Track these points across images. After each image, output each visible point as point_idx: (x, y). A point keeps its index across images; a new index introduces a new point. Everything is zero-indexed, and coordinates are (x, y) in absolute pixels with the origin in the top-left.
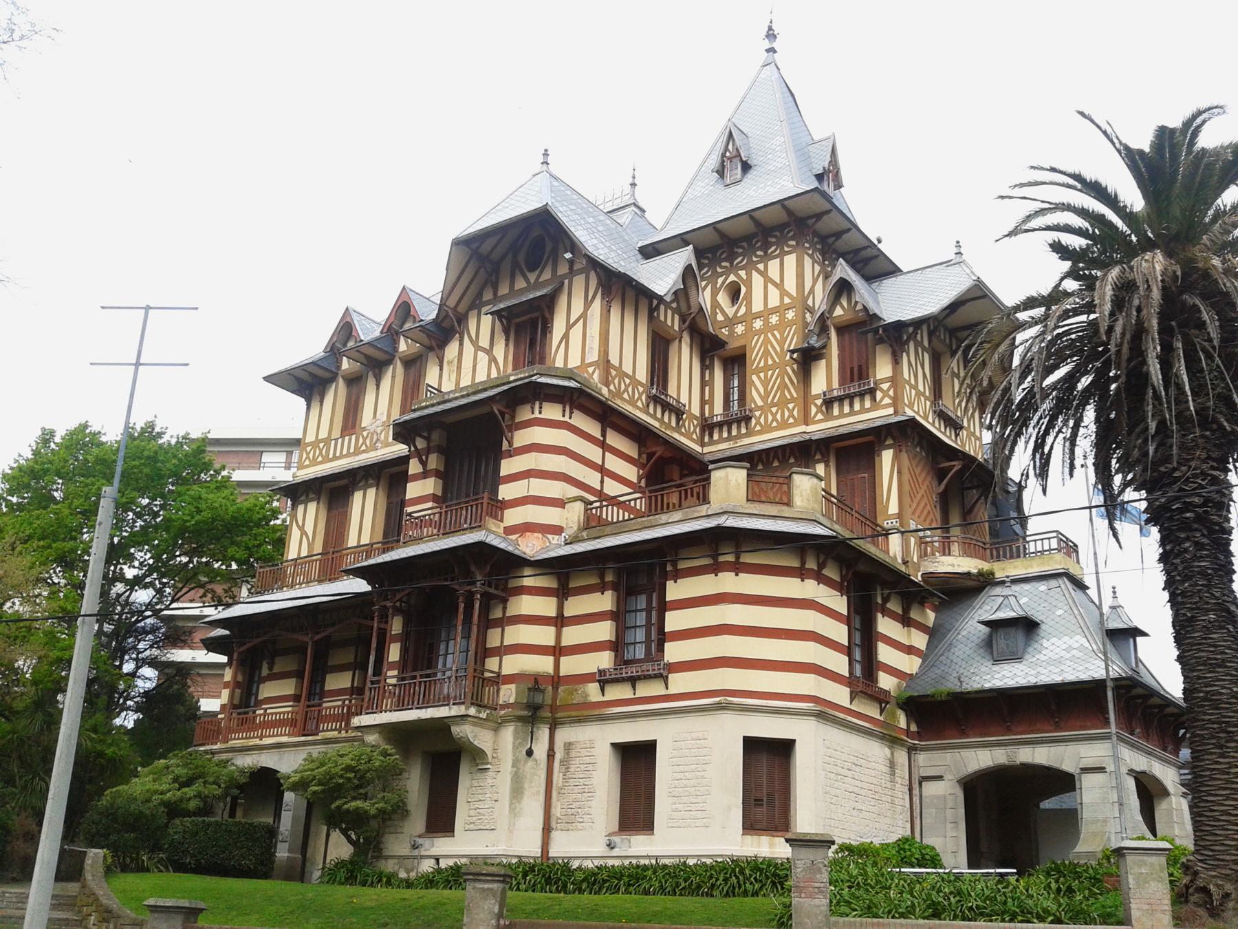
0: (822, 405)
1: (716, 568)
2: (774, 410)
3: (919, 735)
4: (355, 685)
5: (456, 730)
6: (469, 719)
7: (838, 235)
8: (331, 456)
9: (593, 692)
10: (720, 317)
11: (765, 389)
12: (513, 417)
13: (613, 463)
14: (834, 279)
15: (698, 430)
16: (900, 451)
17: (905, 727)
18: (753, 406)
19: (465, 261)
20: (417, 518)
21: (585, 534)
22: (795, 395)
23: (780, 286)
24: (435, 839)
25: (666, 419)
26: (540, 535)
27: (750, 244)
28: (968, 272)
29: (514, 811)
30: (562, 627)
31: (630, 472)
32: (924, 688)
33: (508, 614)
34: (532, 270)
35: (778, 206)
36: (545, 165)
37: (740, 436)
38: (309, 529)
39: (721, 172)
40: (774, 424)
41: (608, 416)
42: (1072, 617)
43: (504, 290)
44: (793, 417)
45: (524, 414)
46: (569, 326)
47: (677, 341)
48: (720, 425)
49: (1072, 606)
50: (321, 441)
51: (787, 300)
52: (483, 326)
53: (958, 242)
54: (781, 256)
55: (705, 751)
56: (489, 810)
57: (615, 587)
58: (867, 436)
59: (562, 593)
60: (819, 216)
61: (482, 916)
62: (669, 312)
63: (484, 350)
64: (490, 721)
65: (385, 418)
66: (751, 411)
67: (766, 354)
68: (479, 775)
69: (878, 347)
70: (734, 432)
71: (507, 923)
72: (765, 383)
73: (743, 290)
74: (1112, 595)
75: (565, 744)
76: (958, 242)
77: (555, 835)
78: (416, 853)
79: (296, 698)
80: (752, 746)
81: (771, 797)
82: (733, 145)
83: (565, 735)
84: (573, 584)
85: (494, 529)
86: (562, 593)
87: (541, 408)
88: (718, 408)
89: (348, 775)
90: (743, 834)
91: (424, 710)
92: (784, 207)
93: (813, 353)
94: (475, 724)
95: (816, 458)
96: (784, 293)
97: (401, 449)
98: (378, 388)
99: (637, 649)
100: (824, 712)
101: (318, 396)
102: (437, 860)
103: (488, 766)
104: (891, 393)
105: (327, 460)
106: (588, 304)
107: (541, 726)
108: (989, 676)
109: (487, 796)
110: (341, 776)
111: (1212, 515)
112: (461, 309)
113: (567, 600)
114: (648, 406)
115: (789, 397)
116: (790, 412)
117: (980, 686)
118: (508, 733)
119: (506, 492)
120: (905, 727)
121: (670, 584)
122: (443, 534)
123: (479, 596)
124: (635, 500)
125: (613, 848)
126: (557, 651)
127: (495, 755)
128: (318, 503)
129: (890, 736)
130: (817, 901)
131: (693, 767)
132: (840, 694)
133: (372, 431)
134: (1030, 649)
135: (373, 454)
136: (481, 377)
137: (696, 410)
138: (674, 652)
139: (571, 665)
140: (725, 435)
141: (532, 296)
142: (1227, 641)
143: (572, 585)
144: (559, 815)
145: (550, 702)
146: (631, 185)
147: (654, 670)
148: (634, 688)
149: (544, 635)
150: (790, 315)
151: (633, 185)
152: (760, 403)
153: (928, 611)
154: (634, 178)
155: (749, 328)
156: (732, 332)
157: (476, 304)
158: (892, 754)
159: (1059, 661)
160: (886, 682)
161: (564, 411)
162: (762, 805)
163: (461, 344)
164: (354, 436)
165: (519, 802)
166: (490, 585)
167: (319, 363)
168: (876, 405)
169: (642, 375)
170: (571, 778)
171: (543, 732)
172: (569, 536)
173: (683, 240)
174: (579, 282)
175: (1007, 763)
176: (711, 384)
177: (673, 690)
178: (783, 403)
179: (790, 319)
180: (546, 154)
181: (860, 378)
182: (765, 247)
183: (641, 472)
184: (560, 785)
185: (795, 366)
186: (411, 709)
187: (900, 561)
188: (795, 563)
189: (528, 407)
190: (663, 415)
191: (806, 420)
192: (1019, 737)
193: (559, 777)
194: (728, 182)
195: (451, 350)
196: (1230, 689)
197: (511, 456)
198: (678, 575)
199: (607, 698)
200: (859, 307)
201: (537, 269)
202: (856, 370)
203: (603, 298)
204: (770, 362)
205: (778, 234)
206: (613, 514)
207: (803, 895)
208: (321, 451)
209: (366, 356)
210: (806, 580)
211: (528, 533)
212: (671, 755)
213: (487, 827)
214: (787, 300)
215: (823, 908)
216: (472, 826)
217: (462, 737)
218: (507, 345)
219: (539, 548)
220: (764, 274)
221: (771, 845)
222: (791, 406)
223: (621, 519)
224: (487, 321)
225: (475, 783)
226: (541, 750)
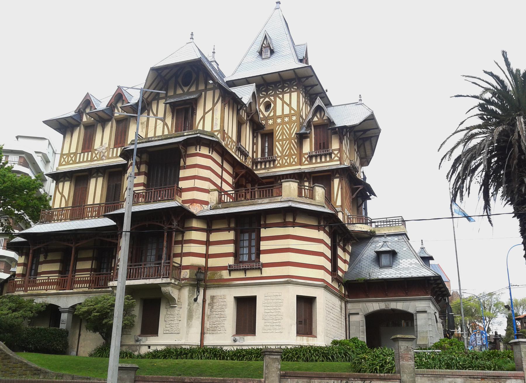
0: (308, 157)
1: (284, 225)
2: (286, 158)
3: (349, 296)
4: (93, 267)
5: (163, 289)
6: (171, 284)
7: (312, 86)
8: (77, 161)
9: (225, 274)
10: (261, 116)
11: (282, 149)
12: (186, 151)
13: (226, 176)
14: (315, 105)
16: (342, 180)
18: (276, 155)
19: (154, 79)
20: (136, 193)
21: (220, 206)
22: (296, 153)
23: (289, 105)
24: (148, 337)
26: (199, 205)
27: (275, 85)
28: (367, 108)
29: (189, 326)
30: (209, 245)
31: (230, 179)
32: (352, 277)
33: (185, 239)
34: (186, 85)
35: (292, 71)
36: (192, 39)
37: (270, 168)
38: (66, 193)
39: (260, 53)
40: (286, 164)
41: (224, 154)
42: (411, 251)
43: (171, 93)
44: (295, 162)
46: (205, 113)
47: (245, 124)
48: (261, 163)
49: (410, 246)
50: (72, 153)
51: (293, 112)
52: (160, 108)
53: (360, 95)
54: (290, 92)
55: (280, 301)
56: (176, 325)
57: (234, 229)
58: (328, 172)
59: (209, 231)
60: (308, 77)
61: (273, 370)
62: (243, 111)
63: (160, 119)
65: (107, 146)
66: (276, 157)
67: (283, 134)
68: (173, 309)
69: (333, 136)
70: (267, 166)
71: (284, 373)
72: (282, 146)
73: (272, 105)
74: (421, 243)
75: (211, 296)
76: (360, 95)
77: (207, 336)
78: (138, 343)
79: (59, 272)
80: (300, 299)
81: (305, 320)
82: (266, 42)
83: (210, 293)
86: (209, 231)
87: (200, 148)
90: (297, 336)
91: (148, 280)
92: (294, 71)
93: (306, 135)
94: (172, 287)
95: (305, 180)
96: (291, 108)
98: (103, 132)
99: (244, 256)
101: (70, 133)
103: (176, 305)
104: (339, 155)
105: (75, 162)
106: (214, 104)
108: (379, 274)
109: (175, 318)
110: (109, 309)
112: (149, 100)
113: (211, 234)
115: (293, 153)
116: (294, 159)
117: (376, 277)
118: (186, 292)
119: (182, 184)
122: (153, 202)
125: (236, 342)
126: (207, 256)
127: (179, 301)
128: (71, 183)
130: (410, 363)
131: (274, 307)
132: (328, 278)
133: (100, 151)
134: (394, 263)
136: (159, 133)
137: (250, 155)
138: (264, 259)
139: (213, 263)
140: (263, 167)
141: (188, 98)
143: (213, 228)
144: (208, 327)
146: (213, 52)
147: (256, 266)
149: (202, 249)
150: (294, 118)
151: (214, 53)
152: (280, 154)
154: (214, 49)
155: (275, 122)
156: (267, 122)
157: (157, 98)
159: (408, 269)
161: (210, 151)
162: (302, 324)
163: (148, 114)
164: (90, 153)
165: (191, 322)
168: (331, 160)
169: (234, 138)
170: (214, 311)
172: (213, 206)
173: (247, 81)
174: (210, 94)
175: (385, 309)
176: (257, 144)
177: (264, 275)
179: (294, 120)
180: (192, 34)
181: (324, 148)
182: (283, 88)
184: (209, 314)
185: (296, 140)
186: (140, 279)
188: (315, 223)
189: (194, 148)
190: (241, 156)
191: (301, 164)
192: (391, 298)
193: (208, 310)
194: (264, 57)
197: (185, 169)
198: (267, 226)
199: (231, 277)
200: (325, 118)
201: (188, 85)
202: (322, 144)
203: (222, 102)
204: (284, 137)
205: (289, 83)
206: (225, 198)
207: (404, 360)
208: (72, 158)
209: (99, 116)
210: (320, 231)
211: (194, 204)
212: (264, 302)
213: (176, 332)
214: (293, 112)
215: (412, 365)
216: (167, 332)
217: (167, 292)
218: (173, 118)
219: (199, 210)
220: (282, 99)
221: (307, 341)
222: (294, 157)
224: (162, 106)
225: (169, 313)
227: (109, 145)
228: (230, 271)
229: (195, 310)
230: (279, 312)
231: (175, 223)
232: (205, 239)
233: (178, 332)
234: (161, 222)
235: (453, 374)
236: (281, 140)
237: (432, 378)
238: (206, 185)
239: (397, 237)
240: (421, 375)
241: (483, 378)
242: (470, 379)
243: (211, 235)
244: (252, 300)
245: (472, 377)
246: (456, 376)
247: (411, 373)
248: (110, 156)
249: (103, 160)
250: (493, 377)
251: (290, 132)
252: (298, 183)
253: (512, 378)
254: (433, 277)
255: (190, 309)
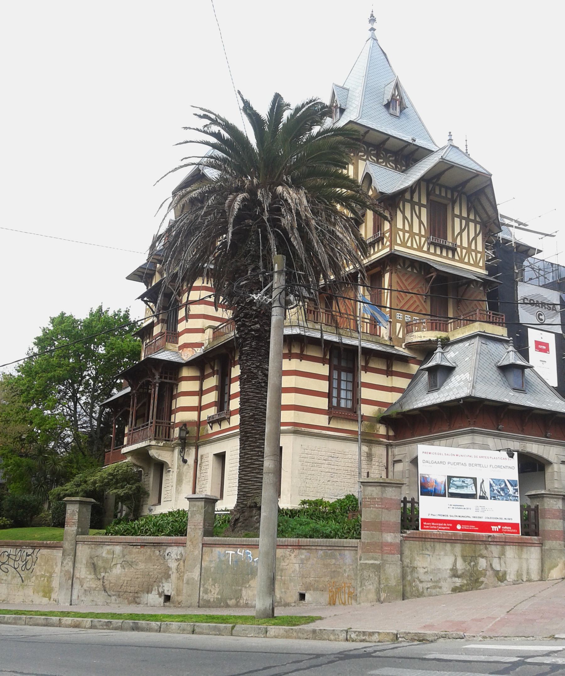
3: (395, 438)
17: (385, 433)
26: (191, 349)
29: (178, 492)
30: (202, 396)
59: (202, 378)
64: (166, 447)
85: (171, 348)
89: (109, 478)
107: (191, 447)
111: (247, 322)
120: (385, 433)
123: (157, 385)
126: (200, 409)
129: (366, 439)
130: (73, 528)
132: (322, 420)
142: (252, 388)
145: (195, 435)
148: (220, 426)
153: (412, 365)
158: (370, 450)
160: (367, 410)
165: (180, 487)
166: (166, 378)
167: (143, 267)
168: (384, 247)
171: (192, 451)
177: (232, 425)
187: (386, 338)
192: (432, 435)
196: (249, 414)
210: (292, 360)
211: (185, 349)
219: (190, 356)
226: (191, 460)
229: (185, 473)
231: (157, 377)
235: (112, 541)
237: (93, 546)
239: (469, 341)
240: (82, 543)
241: (143, 545)
242: (129, 547)
243: (204, 383)
245: (131, 544)
246: (115, 544)
247: (72, 540)
250: (152, 544)
253: (173, 545)
255: (179, 472)
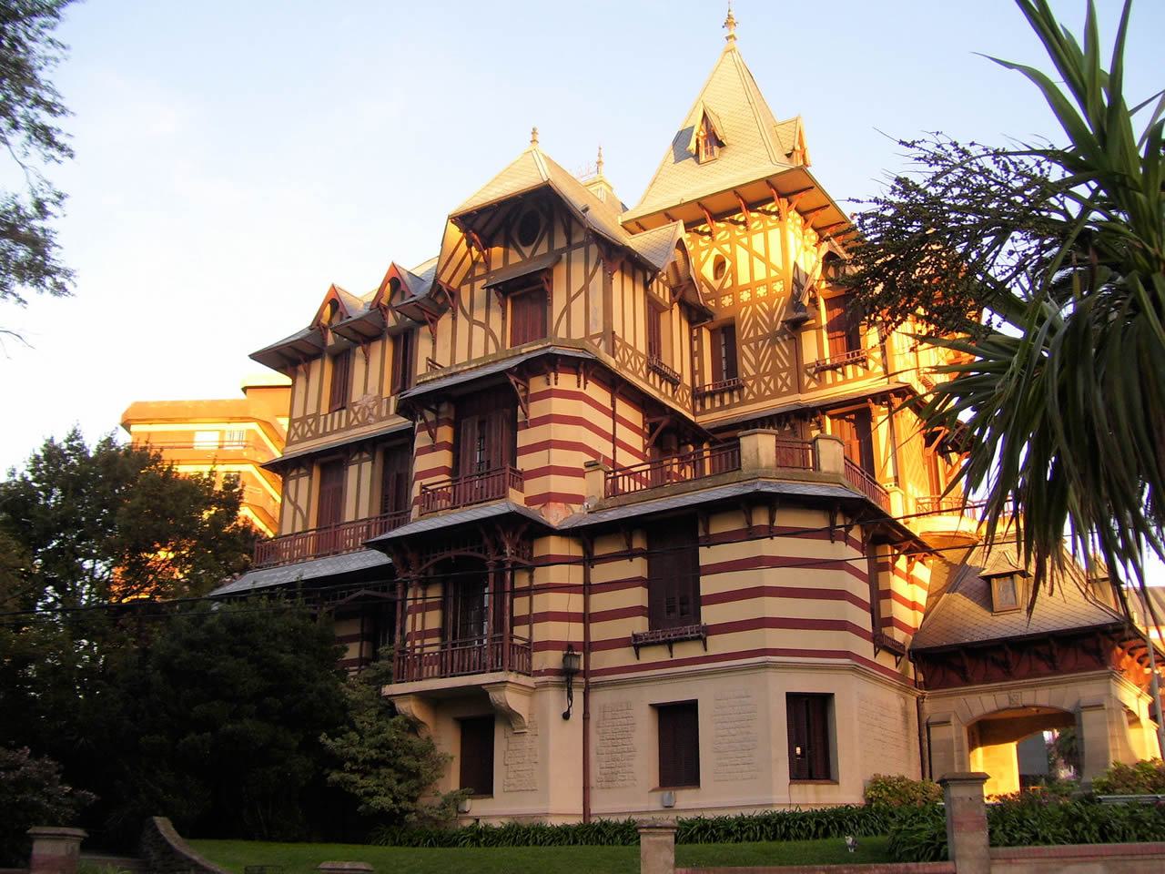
1: (751, 534)
2: (767, 379)
3: (926, 685)
5: (495, 696)
6: (509, 685)
8: (321, 431)
11: (757, 359)
13: (624, 434)
15: (690, 400)
22: (788, 365)
25: (663, 390)
31: (637, 442)
34: (526, 244)
38: (302, 503)
40: (768, 393)
44: (787, 385)
45: (537, 384)
46: (570, 299)
48: (712, 394)
50: (309, 417)
59: (588, 561)
63: (479, 324)
65: (376, 393)
68: (518, 738)
72: (756, 352)
73: (728, 264)
77: (594, 794)
80: (793, 699)
84: (598, 552)
86: (588, 561)
87: (556, 379)
88: (708, 379)
96: (769, 266)
97: (401, 422)
98: (367, 364)
100: (860, 666)
102: (478, 820)
105: (316, 435)
106: (588, 278)
113: (593, 567)
114: (648, 376)
119: (524, 463)
121: (702, 550)
124: (647, 470)
126: (587, 618)
127: (531, 720)
132: (865, 648)
135: (367, 429)
136: (478, 353)
137: (687, 380)
138: (710, 615)
140: (717, 404)
143: (598, 552)
147: (692, 633)
148: (671, 650)
149: (574, 603)
152: (752, 373)
161: (579, 382)
163: (454, 319)
169: (642, 347)
173: (667, 215)
174: (578, 254)
176: (700, 353)
177: (712, 651)
178: (775, 373)
180: (534, 132)
183: (646, 442)
190: (661, 386)
195: (445, 323)
199: (640, 662)
201: (533, 243)
203: (604, 271)
204: (760, 333)
206: (626, 484)
208: (310, 426)
211: (552, 504)
214: (773, 273)
216: (512, 788)
221: (817, 793)
222: (784, 375)
223: (632, 489)
225: (512, 747)
227: (381, 390)
228: (637, 648)
230: (748, 733)
232: (580, 581)
233: (534, 788)
234: (480, 551)
236: (752, 340)
238: (578, 460)
244: (690, 708)
248: (384, 414)
249: (369, 424)
251: (771, 319)
252: (776, 435)
254: (1111, 624)
